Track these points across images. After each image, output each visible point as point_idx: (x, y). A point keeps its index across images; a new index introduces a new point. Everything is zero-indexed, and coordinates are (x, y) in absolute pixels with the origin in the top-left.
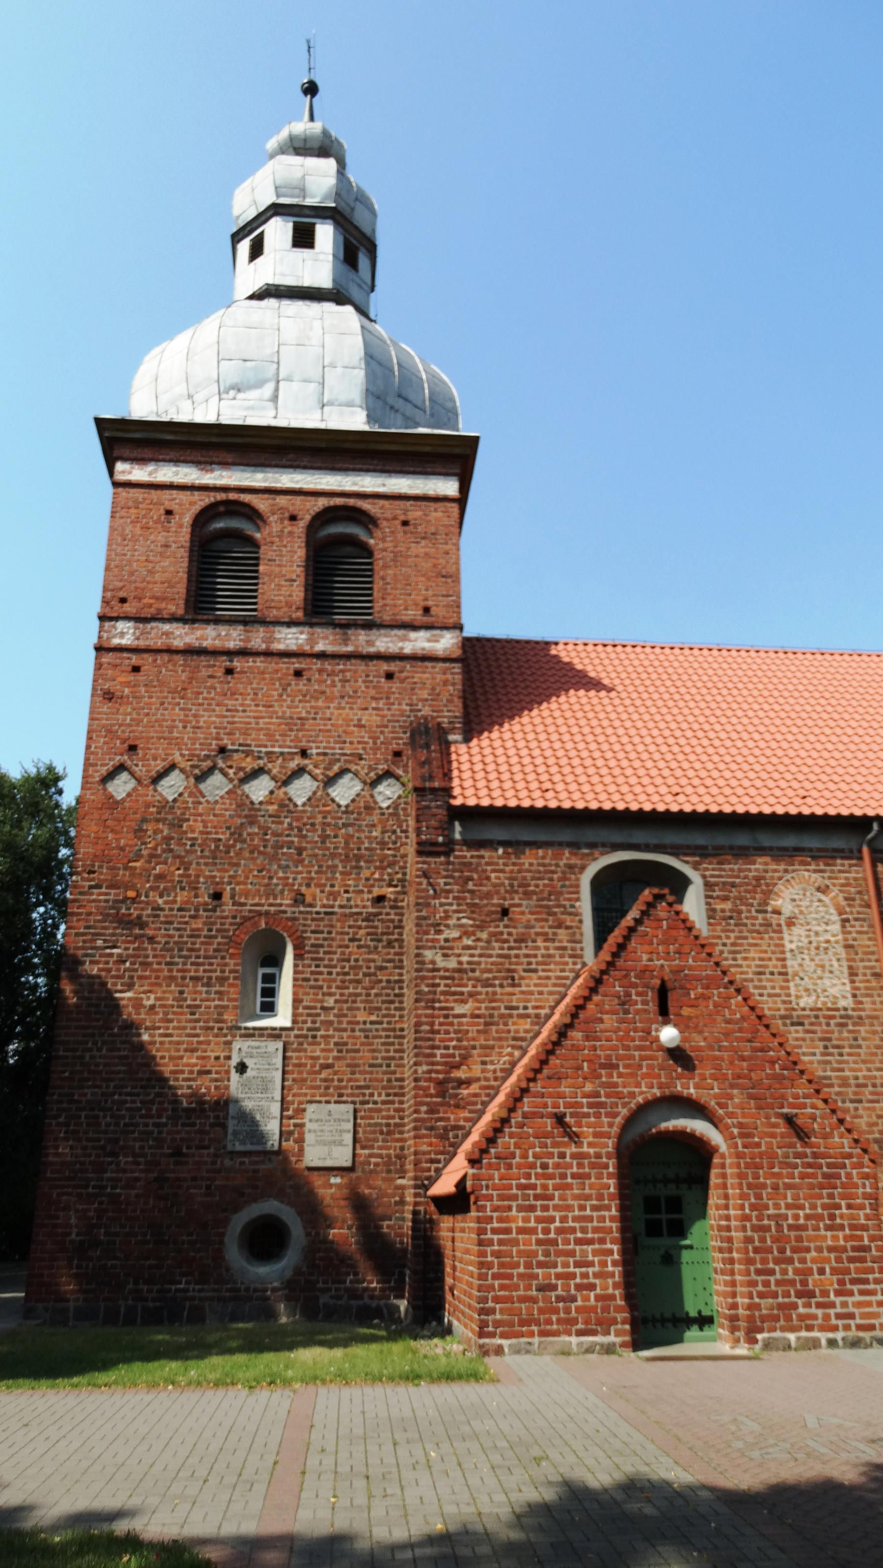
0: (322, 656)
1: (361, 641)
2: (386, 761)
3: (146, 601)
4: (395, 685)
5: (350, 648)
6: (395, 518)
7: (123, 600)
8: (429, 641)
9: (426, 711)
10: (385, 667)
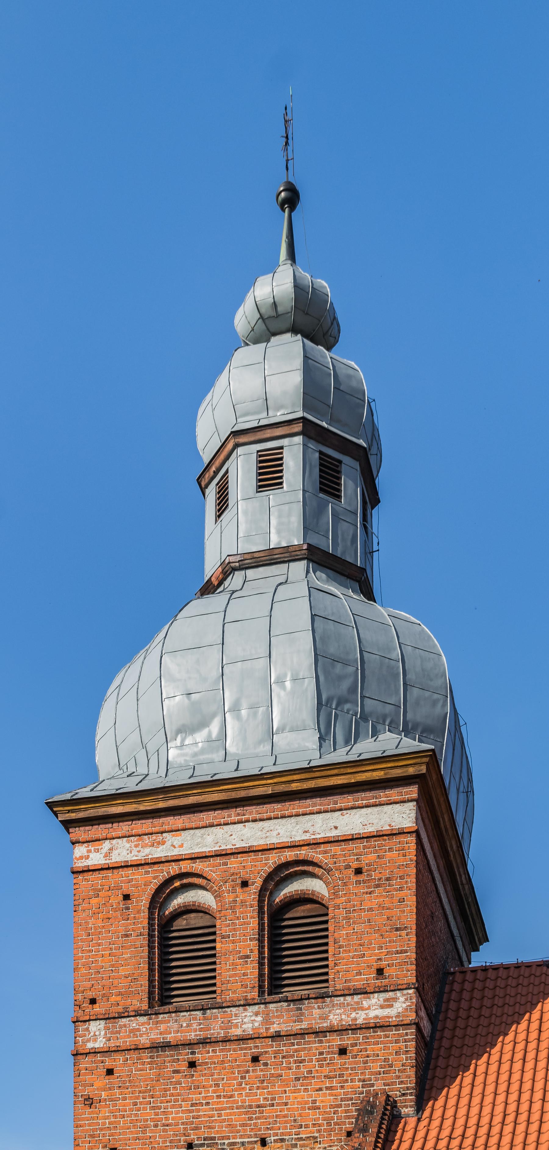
0: (277, 1036)
1: (315, 1015)
2: (340, 1141)
3: (113, 999)
4: (348, 1060)
5: (304, 1025)
6: (348, 867)
7: (93, 1001)
8: (382, 1007)
9: (379, 1086)
10: (336, 1041)
